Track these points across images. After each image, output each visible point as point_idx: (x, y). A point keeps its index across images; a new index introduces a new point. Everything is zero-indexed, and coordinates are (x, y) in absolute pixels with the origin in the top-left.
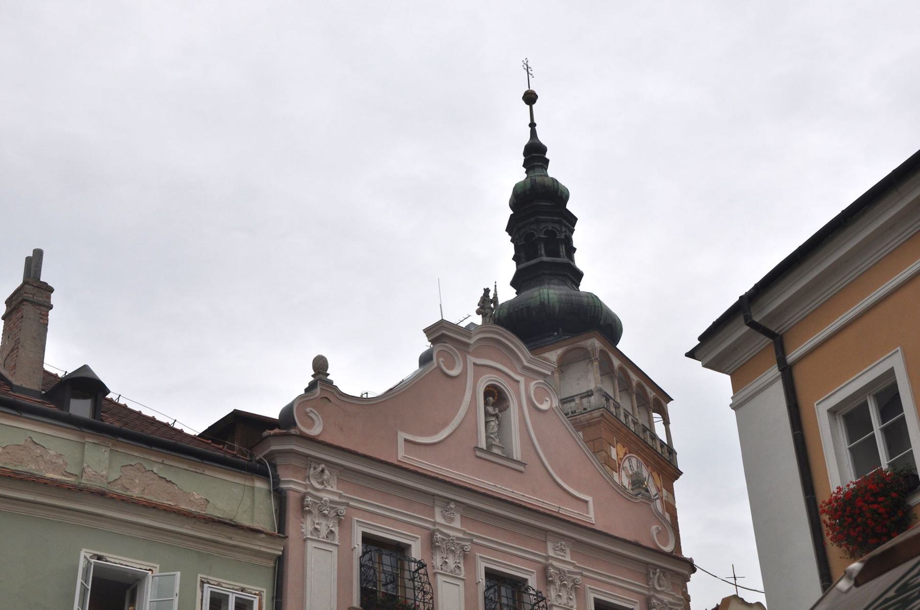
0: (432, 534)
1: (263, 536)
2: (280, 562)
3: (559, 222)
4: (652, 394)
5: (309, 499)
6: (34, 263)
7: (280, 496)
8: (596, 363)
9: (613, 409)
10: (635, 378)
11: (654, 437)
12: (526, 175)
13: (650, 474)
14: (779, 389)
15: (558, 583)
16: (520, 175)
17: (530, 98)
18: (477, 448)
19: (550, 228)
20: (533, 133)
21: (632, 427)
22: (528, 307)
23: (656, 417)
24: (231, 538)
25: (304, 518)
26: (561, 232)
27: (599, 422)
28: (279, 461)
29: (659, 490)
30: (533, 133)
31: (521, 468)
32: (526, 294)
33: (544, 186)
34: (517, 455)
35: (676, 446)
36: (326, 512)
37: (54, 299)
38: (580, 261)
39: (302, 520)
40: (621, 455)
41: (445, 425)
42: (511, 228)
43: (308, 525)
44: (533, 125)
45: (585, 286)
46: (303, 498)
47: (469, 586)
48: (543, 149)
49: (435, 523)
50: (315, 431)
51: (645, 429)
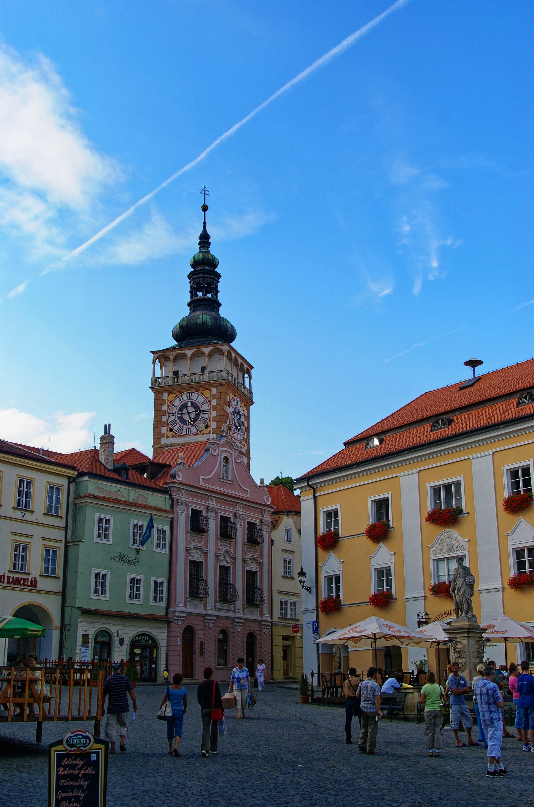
0: (208, 507)
2: (172, 519)
3: (213, 279)
4: (246, 366)
5: (179, 501)
6: (107, 428)
7: (172, 499)
8: (225, 358)
9: (230, 378)
10: (240, 361)
11: (245, 387)
12: (199, 250)
14: (312, 501)
15: (239, 518)
17: (205, 209)
18: (220, 478)
19: (209, 281)
22: (196, 323)
26: (213, 284)
27: (224, 385)
28: (171, 489)
31: (231, 483)
33: (208, 259)
34: (230, 479)
35: (253, 390)
38: (221, 298)
40: (231, 398)
41: (212, 472)
42: (190, 276)
44: (205, 223)
45: (223, 312)
46: (178, 500)
47: (217, 520)
49: (209, 504)
50: (180, 479)
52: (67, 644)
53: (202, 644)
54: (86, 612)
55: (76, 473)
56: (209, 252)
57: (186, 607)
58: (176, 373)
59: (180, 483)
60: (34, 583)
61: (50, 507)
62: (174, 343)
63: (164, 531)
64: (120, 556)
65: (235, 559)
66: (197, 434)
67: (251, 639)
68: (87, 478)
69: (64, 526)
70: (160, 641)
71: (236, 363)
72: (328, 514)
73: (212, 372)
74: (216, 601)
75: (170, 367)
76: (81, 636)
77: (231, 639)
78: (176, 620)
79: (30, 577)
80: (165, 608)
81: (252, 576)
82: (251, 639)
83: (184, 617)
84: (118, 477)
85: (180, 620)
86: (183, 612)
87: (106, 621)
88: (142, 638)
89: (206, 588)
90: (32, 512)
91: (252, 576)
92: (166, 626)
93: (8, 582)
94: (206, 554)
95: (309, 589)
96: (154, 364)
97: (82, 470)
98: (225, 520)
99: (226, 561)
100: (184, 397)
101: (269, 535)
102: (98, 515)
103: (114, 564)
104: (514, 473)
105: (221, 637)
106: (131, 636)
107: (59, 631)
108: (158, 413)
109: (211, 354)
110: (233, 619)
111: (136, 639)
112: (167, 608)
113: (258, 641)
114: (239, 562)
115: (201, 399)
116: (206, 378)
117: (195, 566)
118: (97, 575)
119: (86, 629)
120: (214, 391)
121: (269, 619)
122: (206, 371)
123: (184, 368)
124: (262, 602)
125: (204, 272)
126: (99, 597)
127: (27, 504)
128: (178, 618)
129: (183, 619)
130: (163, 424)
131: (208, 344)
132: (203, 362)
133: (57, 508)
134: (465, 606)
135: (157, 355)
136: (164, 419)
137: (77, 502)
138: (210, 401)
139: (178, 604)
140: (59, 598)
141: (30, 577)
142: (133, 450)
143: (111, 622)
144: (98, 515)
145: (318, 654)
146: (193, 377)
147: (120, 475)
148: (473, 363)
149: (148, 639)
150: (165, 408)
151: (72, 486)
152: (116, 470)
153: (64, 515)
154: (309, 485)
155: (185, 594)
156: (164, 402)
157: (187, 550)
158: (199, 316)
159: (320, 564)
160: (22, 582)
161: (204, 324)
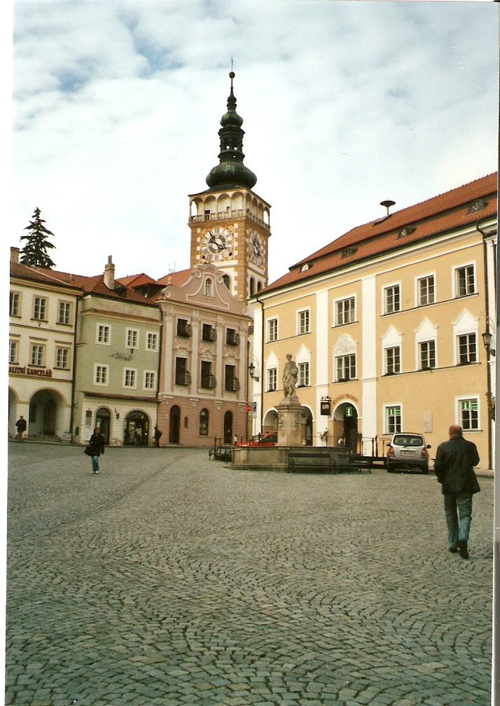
2: (162, 326)
4: (264, 206)
6: (110, 258)
7: (162, 312)
8: (245, 200)
10: (259, 201)
11: (263, 223)
13: (260, 237)
16: (224, 111)
17: (232, 75)
20: (232, 91)
21: (255, 221)
22: (224, 172)
23: (265, 213)
29: (263, 242)
30: (232, 91)
32: (223, 164)
33: (233, 118)
37: (115, 268)
38: (244, 151)
42: (221, 132)
44: (232, 88)
47: (199, 327)
48: (235, 100)
50: (168, 297)
51: (260, 220)
52: (75, 417)
53: (186, 419)
54: (89, 395)
55: (83, 293)
56: (235, 113)
57: (173, 392)
58: (207, 212)
59: (168, 300)
60: (49, 374)
61: (61, 319)
62: (207, 188)
63: (155, 336)
65: (215, 356)
66: (223, 260)
67: (229, 417)
68: (89, 296)
69: (73, 332)
71: (255, 203)
72: (271, 322)
73: (235, 211)
74: (198, 388)
75: (203, 208)
77: (211, 415)
79: (46, 370)
81: (230, 370)
82: (229, 417)
84: (117, 296)
86: (170, 395)
89: (190, 378)
90: (47, 322)
91: (230, 370)
92: (156, 405)
93: (28, 373)
94: (190, 352)
95: (257, 379)
96: (191, 205)
97: (88, 290)
98: (207, 329)
99: (208, 358)
100: (213, 231)
101: (246, 338)
102: (99, 324)
103: (113, 360)
104: (389, 291)
105: (203, 414)
107: (70, 409)
108: (194, 244)
109: (235, 196)
110: (213, 401)
112: (158, 392)
113: (234, 418)
114: (219, 359)
115: (226, 233)
116: (230, 216)
117: (181, 363)
118: (99, 368)
120: (236, 225)
121: (245, 401)
122: (230, 211)
123: (213, 207)
124: (239, 388)
125: (230, 129)
126: (100, 384)
127: (42, 316)
130: (198, 253)
131: (231, 189)
132: (227, 203)
133: (67, 319)
134: (290, 390)
135: (193, 198)
136: (198, 248)
137: (83, 314)
138: (233, 234)
139: (165, 389)
140: (70, 385)
141: (46, 370)
142: (143, 274)
143: (110, 402)
144: (99, 324)
145: (262, 427)
146: (220, 215)
147: (120, 295)
148: (388, 204)
150: (199, 240)
151: (80, 303)
152: (115, 291)
153: (74, 324)
154: (258, 301)
155: (172, 381)
156: (198, 235)
157: (174, 350)
158: (225, 166)
159: (265, 360)
160: (39, 373)
161: (229, 172)
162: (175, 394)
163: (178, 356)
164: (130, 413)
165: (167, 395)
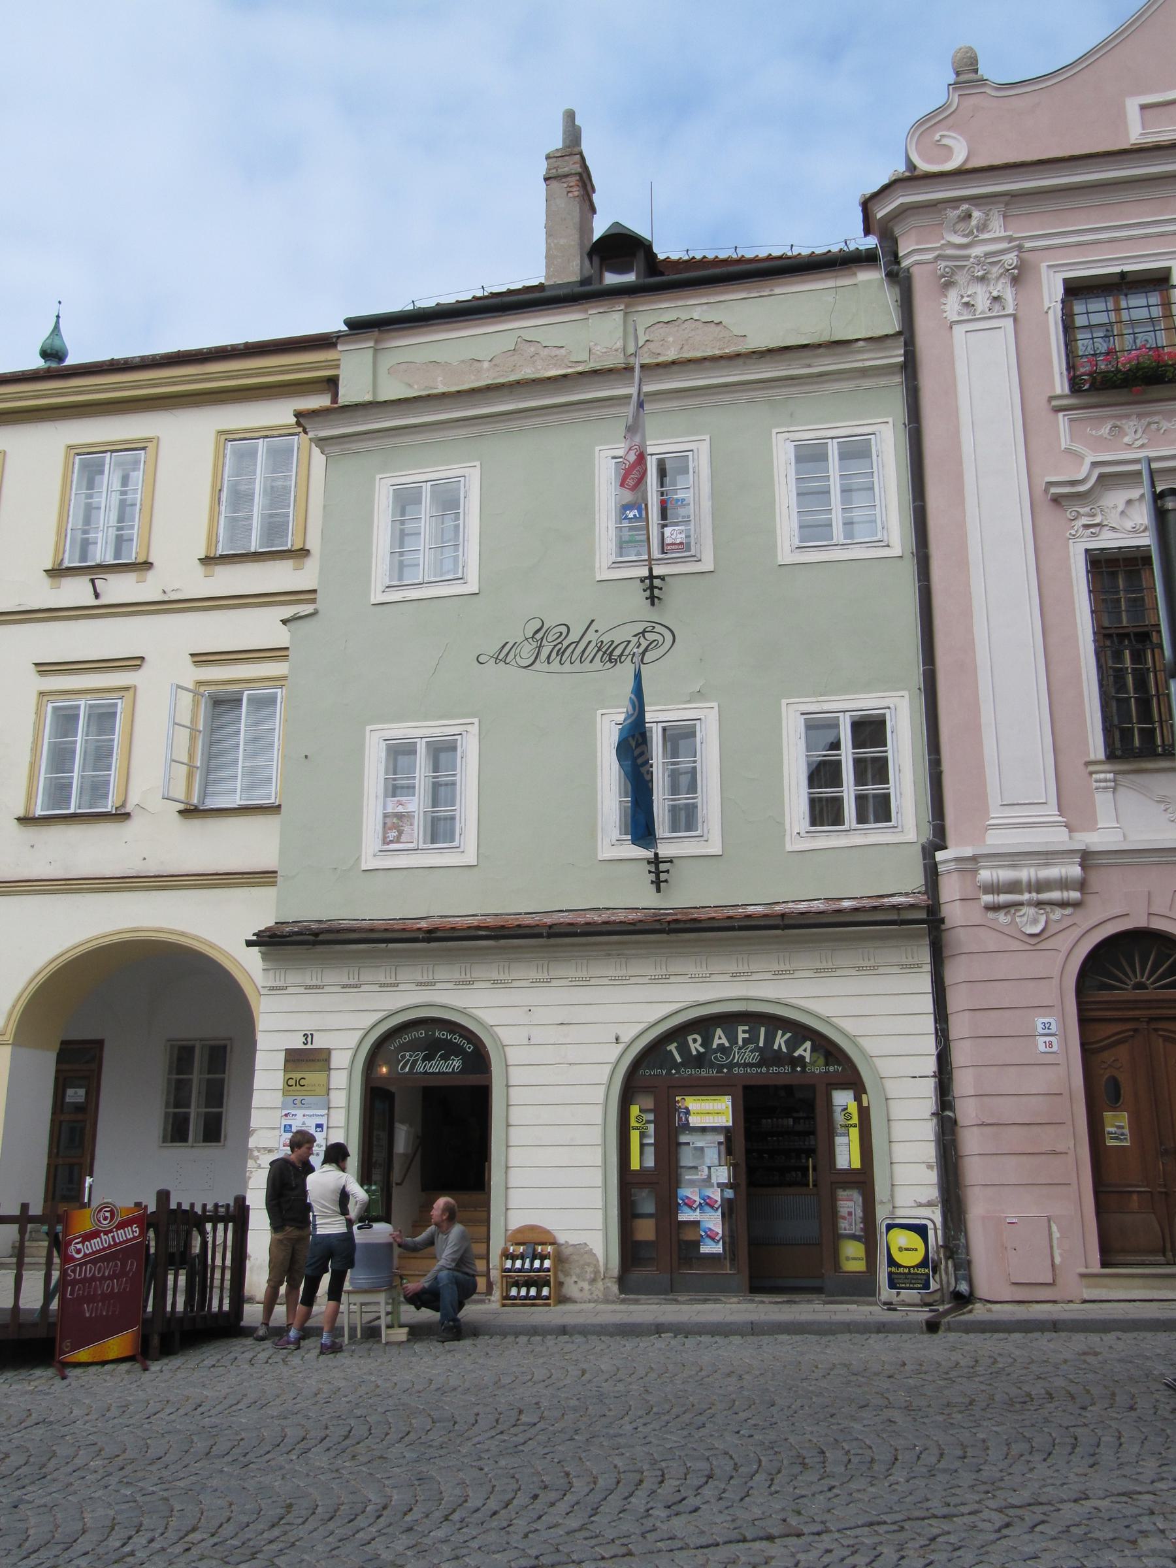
1: (861, 343)
24: (810, 366)
25: (946, 296)
36: (980, 274)
39: (943, 300)
43: (952, 305)
64: (539, 635)
70: (870, 1046)
76: (281, 1057)
78: (995, 908)
80: (917, 851)
83: (1063, 884)
85: (1039, 904)
86: (1048, 856)
87: (443, 972)
88: (733, 1039)
106: (626, 1038)
111: (684, 1049)
119: (308, 1023)
128: (1003, 898)
129: (1055, 895)
139: (997, 815)
149: (781, 1041)
162: (1096, 840)
163: (1108, 540)
164: (679, 1033)
165: (1015, 858)
